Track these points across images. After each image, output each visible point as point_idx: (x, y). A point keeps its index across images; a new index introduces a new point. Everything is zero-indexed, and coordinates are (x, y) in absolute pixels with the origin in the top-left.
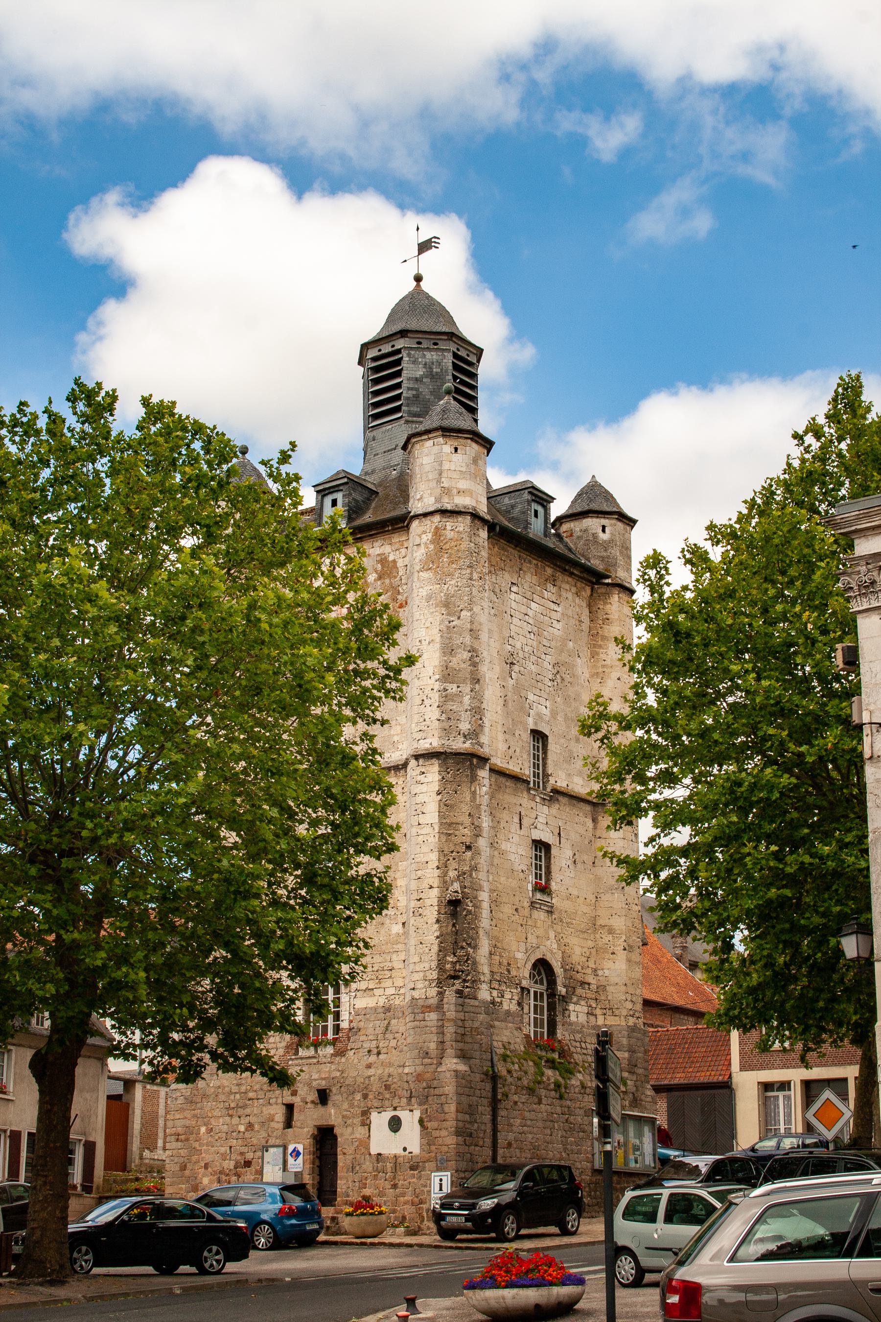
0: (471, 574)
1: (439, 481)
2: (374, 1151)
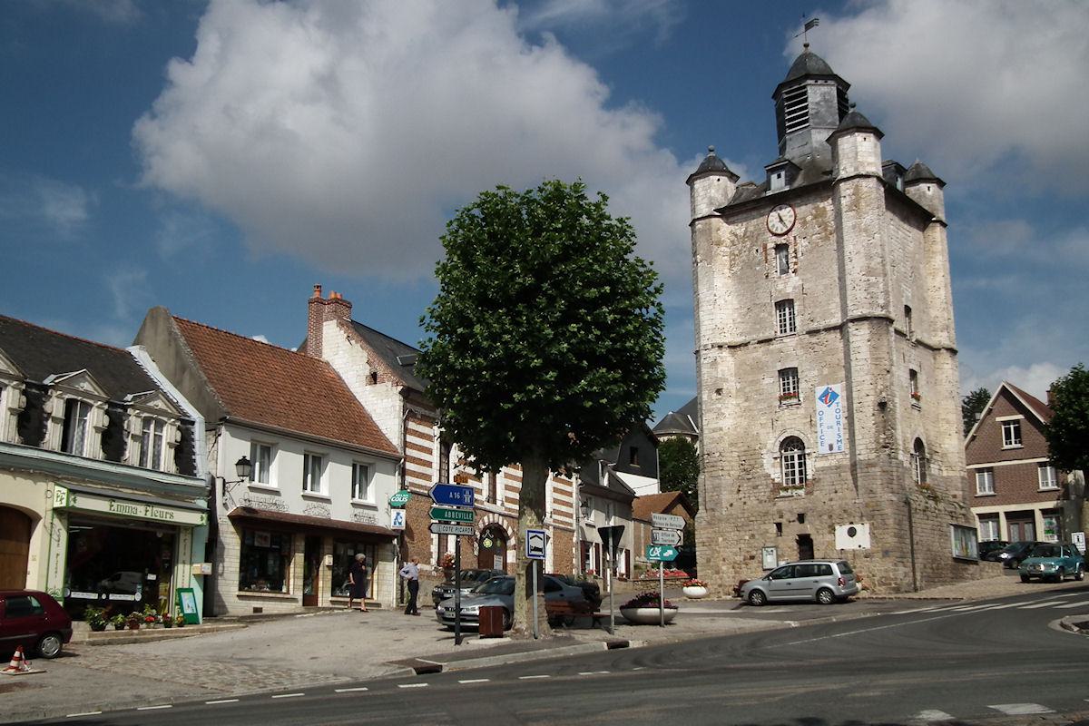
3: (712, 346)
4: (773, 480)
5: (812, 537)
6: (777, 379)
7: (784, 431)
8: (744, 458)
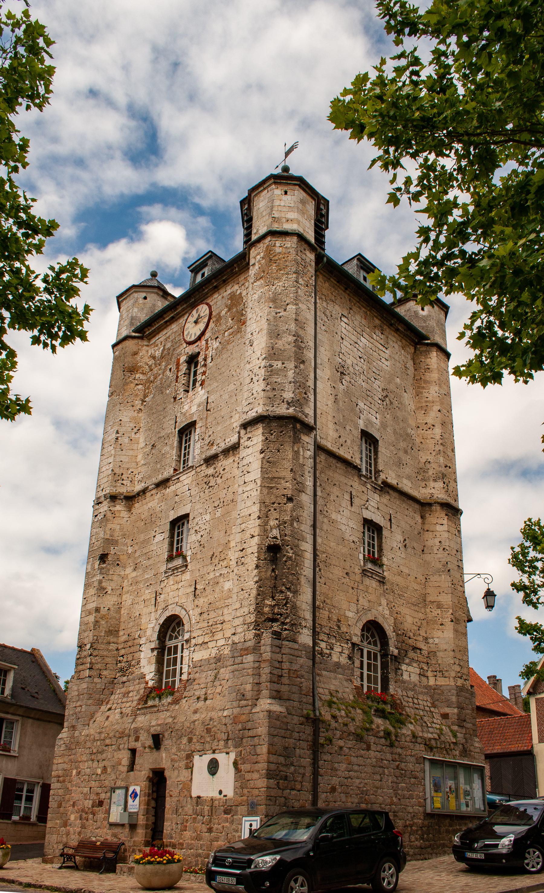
2: (194, 794)
3: (105, 497)
4: (147, 683)
5: (167, 774)
6: (167, 534)
7: (165, 608)
8: (122, 652)
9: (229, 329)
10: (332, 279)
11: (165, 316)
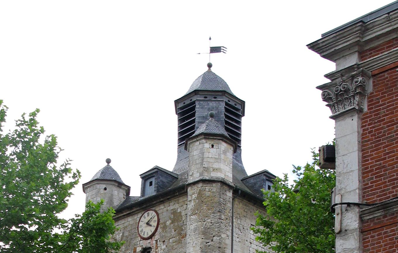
0: (220, 216)
1: (202, 164)
9: (172, 238)
10: (244, 200)
11: (123, 211)
